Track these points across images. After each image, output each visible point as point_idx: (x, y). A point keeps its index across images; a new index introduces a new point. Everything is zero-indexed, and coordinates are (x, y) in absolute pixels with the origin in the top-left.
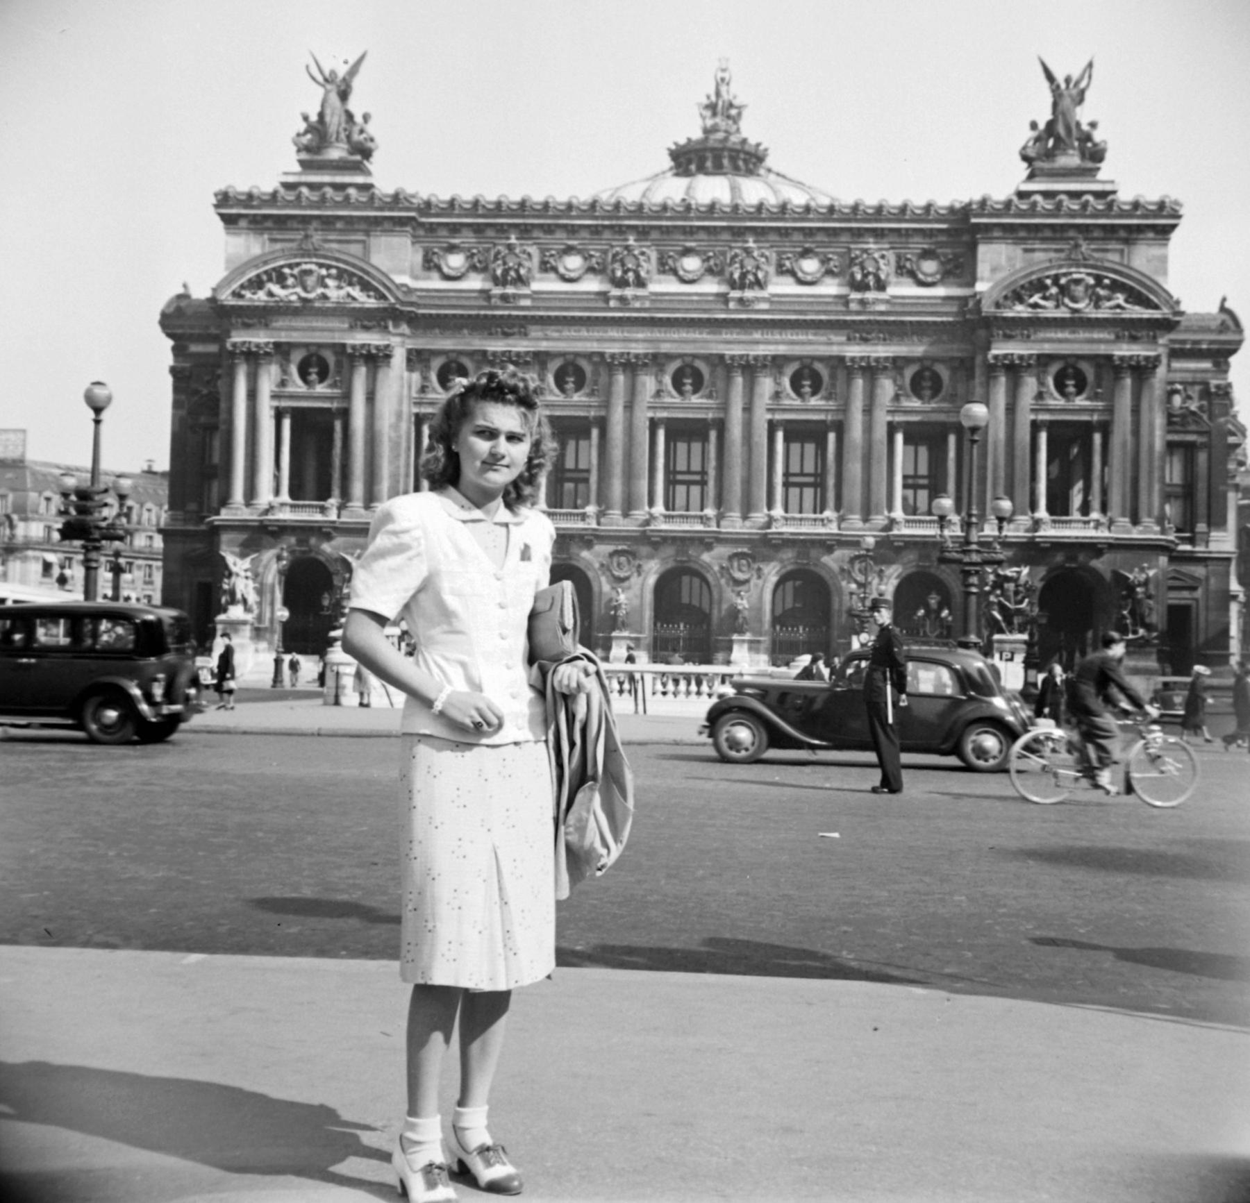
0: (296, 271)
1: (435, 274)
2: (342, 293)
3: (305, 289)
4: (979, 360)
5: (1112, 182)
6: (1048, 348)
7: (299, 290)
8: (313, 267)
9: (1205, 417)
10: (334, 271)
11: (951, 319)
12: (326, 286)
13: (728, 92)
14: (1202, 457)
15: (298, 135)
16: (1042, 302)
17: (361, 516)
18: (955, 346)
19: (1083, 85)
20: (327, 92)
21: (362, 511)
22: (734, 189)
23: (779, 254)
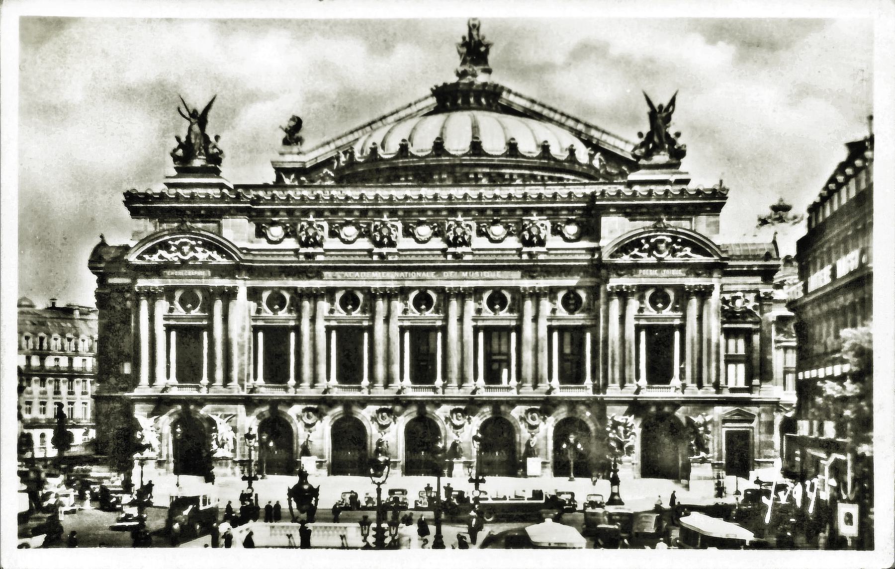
0: (177, 243)
1: (264, 240)
2: (206, 255)
3: (183, 254)
4: (602, 288)
5: (687, 173)
6: (644, 281)
7: (179, 254)
8: (188, 240)
9: (758, 313)
10: (200, 242)
11: (585, 263)
12: (196, 252)
13: (478, 35)
14: (756, 338)
15: (175, 150)
16: (639, 254)
17: (221, 391)
18: (588, 280)
19: (671, 109)
20: (192, 124)
21: (222, 389)
22: (475, 128)
23: (478, 224)
